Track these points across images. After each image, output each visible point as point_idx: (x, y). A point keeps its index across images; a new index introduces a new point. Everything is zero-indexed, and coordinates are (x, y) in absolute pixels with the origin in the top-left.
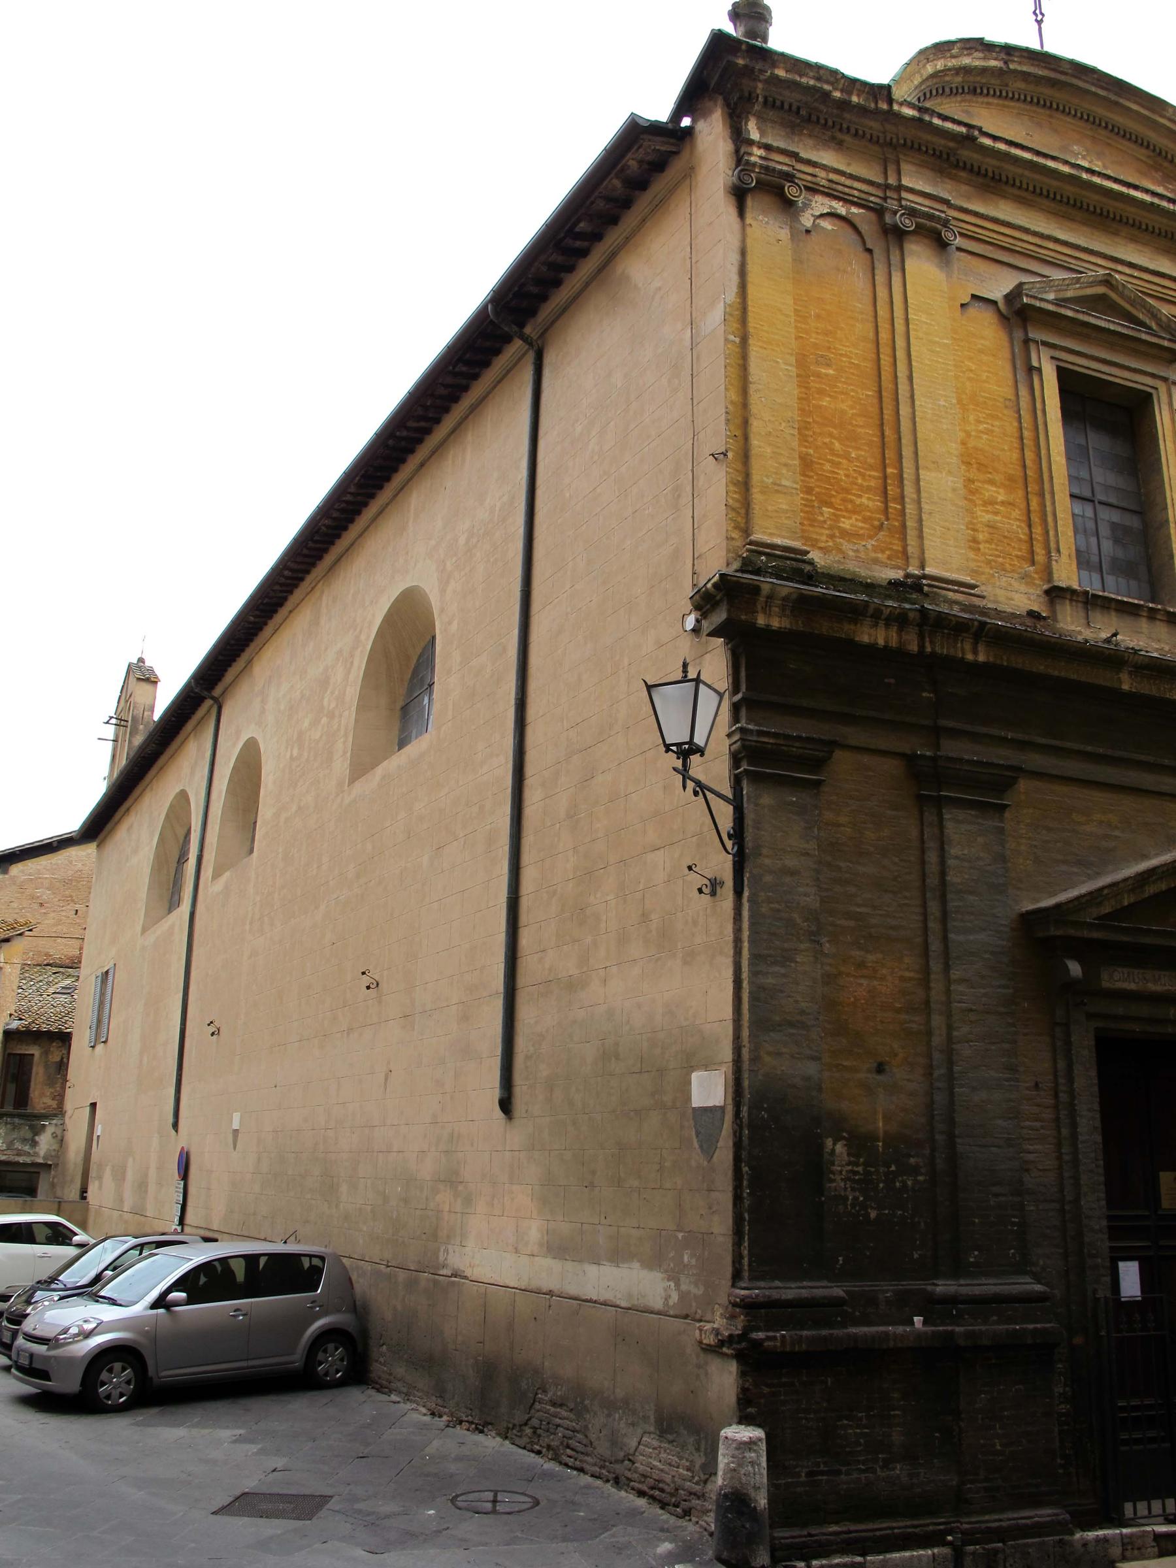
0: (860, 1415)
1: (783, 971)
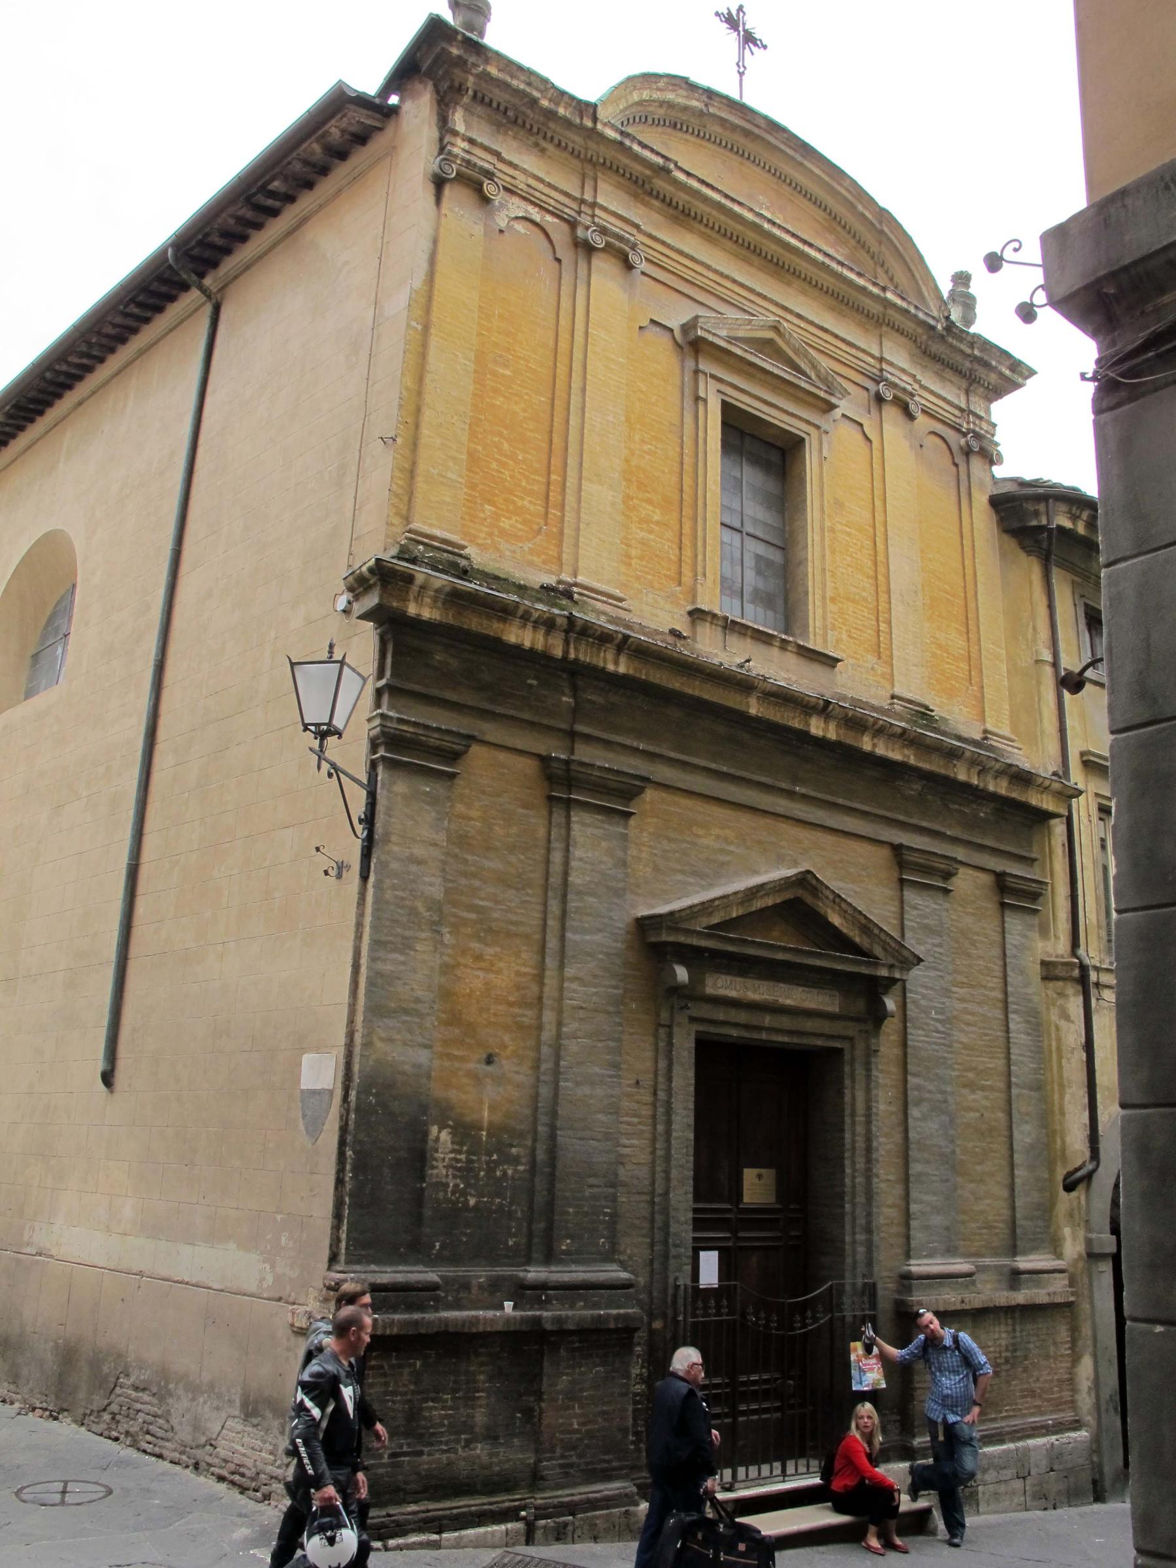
1: (401, 958)
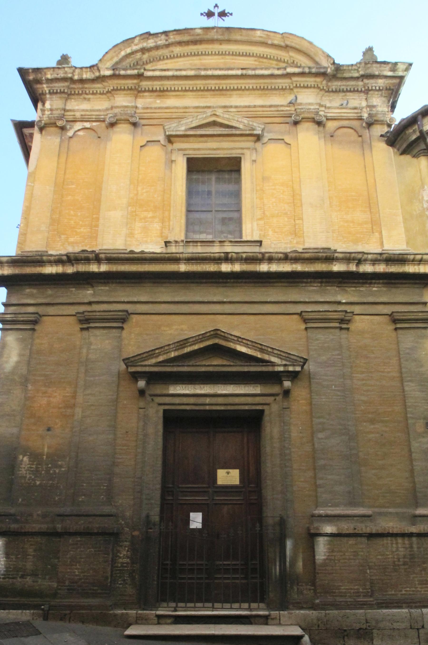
0: (12, 557)
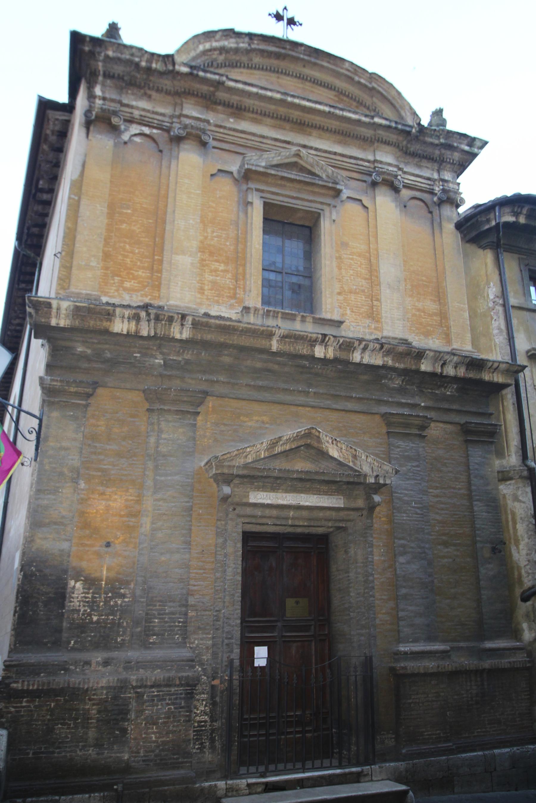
1: (53, 497)
